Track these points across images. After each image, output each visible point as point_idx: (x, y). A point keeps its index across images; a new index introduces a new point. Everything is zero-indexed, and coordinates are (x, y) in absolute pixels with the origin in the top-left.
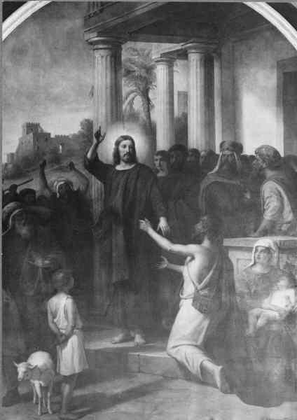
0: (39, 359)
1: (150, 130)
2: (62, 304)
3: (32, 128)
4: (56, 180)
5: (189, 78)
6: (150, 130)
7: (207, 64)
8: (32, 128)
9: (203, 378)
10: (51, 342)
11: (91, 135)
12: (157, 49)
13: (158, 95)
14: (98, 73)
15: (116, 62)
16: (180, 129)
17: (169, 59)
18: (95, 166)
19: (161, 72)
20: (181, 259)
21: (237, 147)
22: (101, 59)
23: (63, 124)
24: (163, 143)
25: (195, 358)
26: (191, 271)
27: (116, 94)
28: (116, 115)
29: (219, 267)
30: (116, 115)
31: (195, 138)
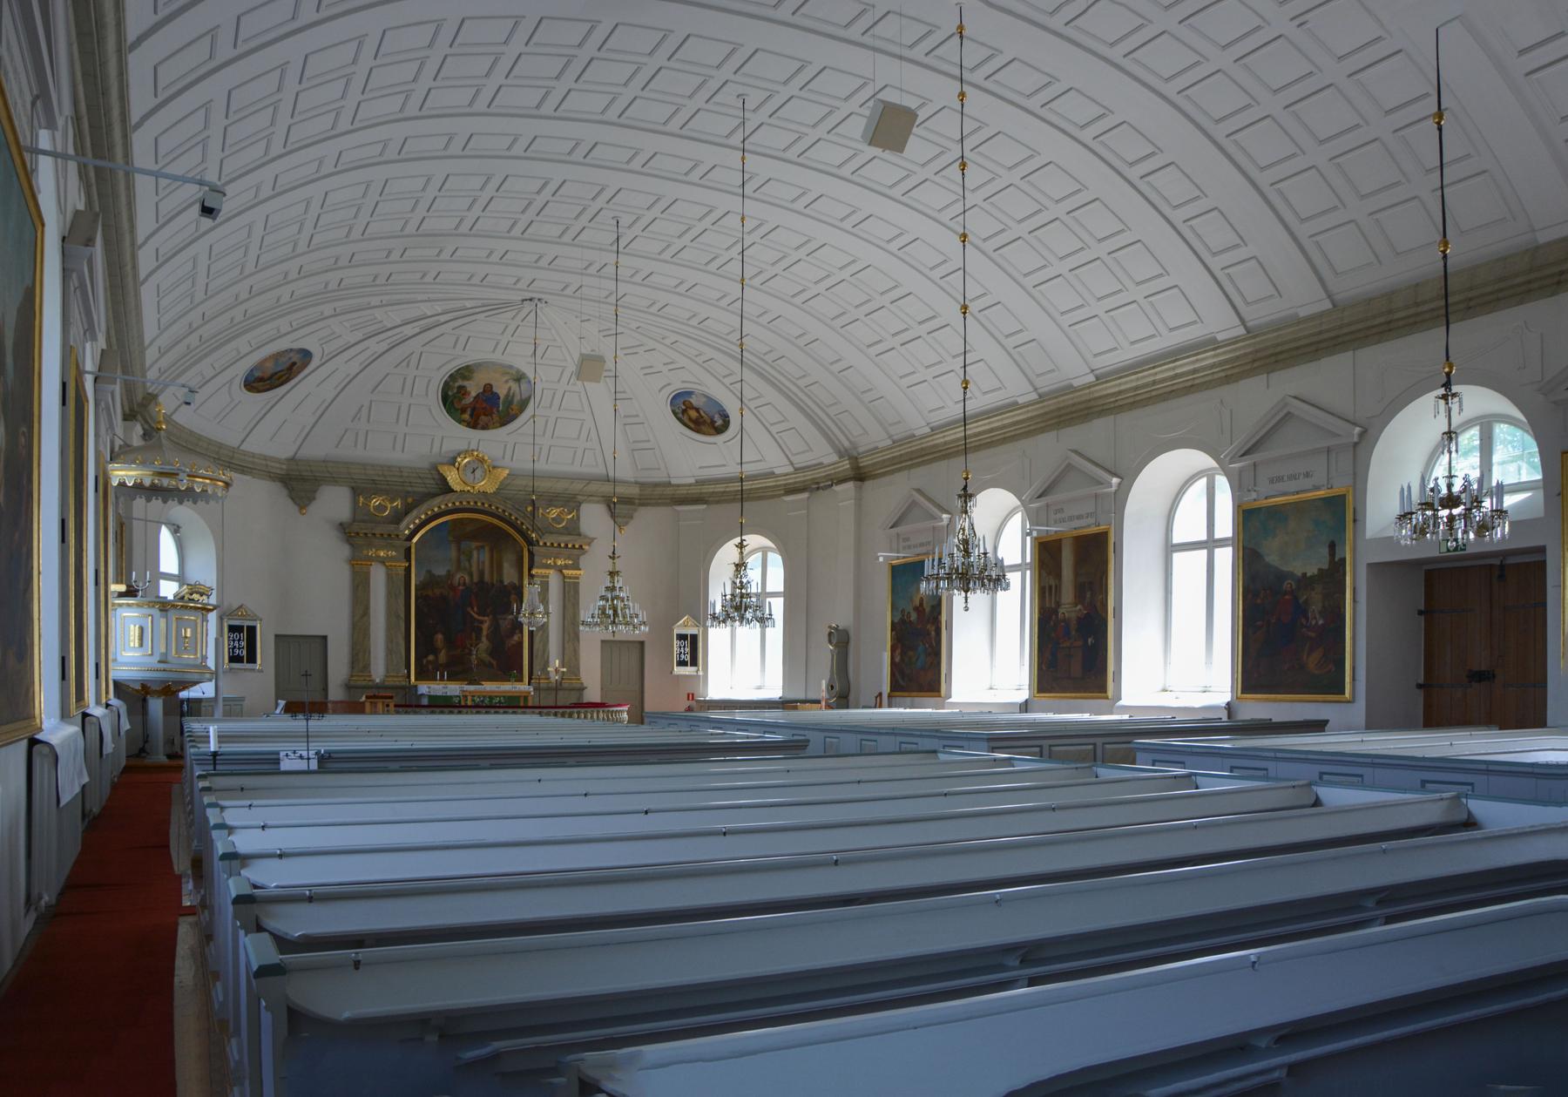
0: (431, 658)
1: (471, 575)
2: (440, 637)
3: (429, 572)
4: (437, 591)
5: (485, 556)
6: (471, 575)
7: (491, 551)
8: (429, 572)
10: (436, 652)
11: (450, 575)
12: (474, 545)
15: (459, 549)
16: (482, 573)
17: (478, 548)
18: (453, 588)
22: (453, 546)
23: (440, 571)
24: (476, 579)
25: (485, 657)
26: (485, 626)
27: (459, 561)
28: (459, 568)
29: (495, 628)
30: (459, 568)
31: (487, 578)
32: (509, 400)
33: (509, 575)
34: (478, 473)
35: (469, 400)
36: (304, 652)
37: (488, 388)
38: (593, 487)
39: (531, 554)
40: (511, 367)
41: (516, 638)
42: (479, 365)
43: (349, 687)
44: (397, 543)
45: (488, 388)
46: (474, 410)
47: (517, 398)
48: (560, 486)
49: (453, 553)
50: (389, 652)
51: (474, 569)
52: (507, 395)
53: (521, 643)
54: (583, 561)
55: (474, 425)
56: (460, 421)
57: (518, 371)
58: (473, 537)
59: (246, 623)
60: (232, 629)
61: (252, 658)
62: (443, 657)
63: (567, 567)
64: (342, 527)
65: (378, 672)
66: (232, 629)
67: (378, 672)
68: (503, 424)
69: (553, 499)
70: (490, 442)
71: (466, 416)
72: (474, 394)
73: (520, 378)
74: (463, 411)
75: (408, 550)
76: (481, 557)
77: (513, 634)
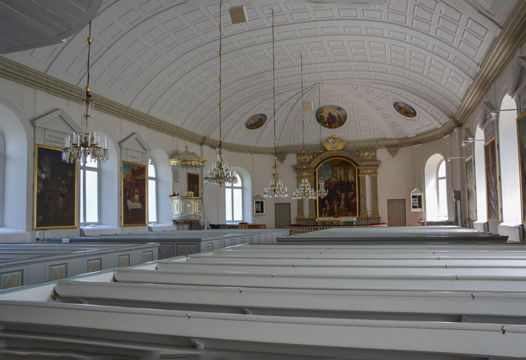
0: (324, 209)
1: (337, 179)
5: (342, 172)
6: (337, 179)
7: (344, 170)
9: (345, 211)
10: (325, 206)
11: (330, 180)
12: (338, 168)
13: (338, 174)
14: (331, 172)
16: (341, 178)
17: (339, 169)
18: (331, 184)
19: (338, 171)
20: (341, 195)
21: (348, 180)
22: (331, 170)
24: (339, 180)
26: (343, 197)
27: (333, 175)
28: (333, 177)
30: (333, 177)
31: (343, 180)
32: (340, 118)
33: (351, 178)
35: (326, 119)
36: (282, 208)
37: (330, 114)
39: (358, 170)
40: (334, 106)
41: (354, 200)
42: (323, 107)
43: (297, 220)
44: (310, 170)
45: (330, 114)
46: (329, 122)
47: (342, 116)
48: (367, 144)
49: (331, 172)
50: (310, 207)
51: (338, 177)
52: (338, 115)
53: (356, 202)
54: (378, 171)
55: (331, 127)
56: (326, 127)
57: (338, 107)
58: (338, 165)
59: (260, 200)
60: (257, 202)
61: (262, 212)
62: (328, 208)
63: (372, 173)
64: (294, 167)
65: (306, 214)
66: (257, 202)
67: (306, 214)
68: (341, 125)
69: (365, 149)
70: (338, 132)
71: (327, 125)
72: (326, 117)
73: (339, 109)
74: (326, 123)
75: (315, 172)
76: (340, 172)
77: (353, 199)
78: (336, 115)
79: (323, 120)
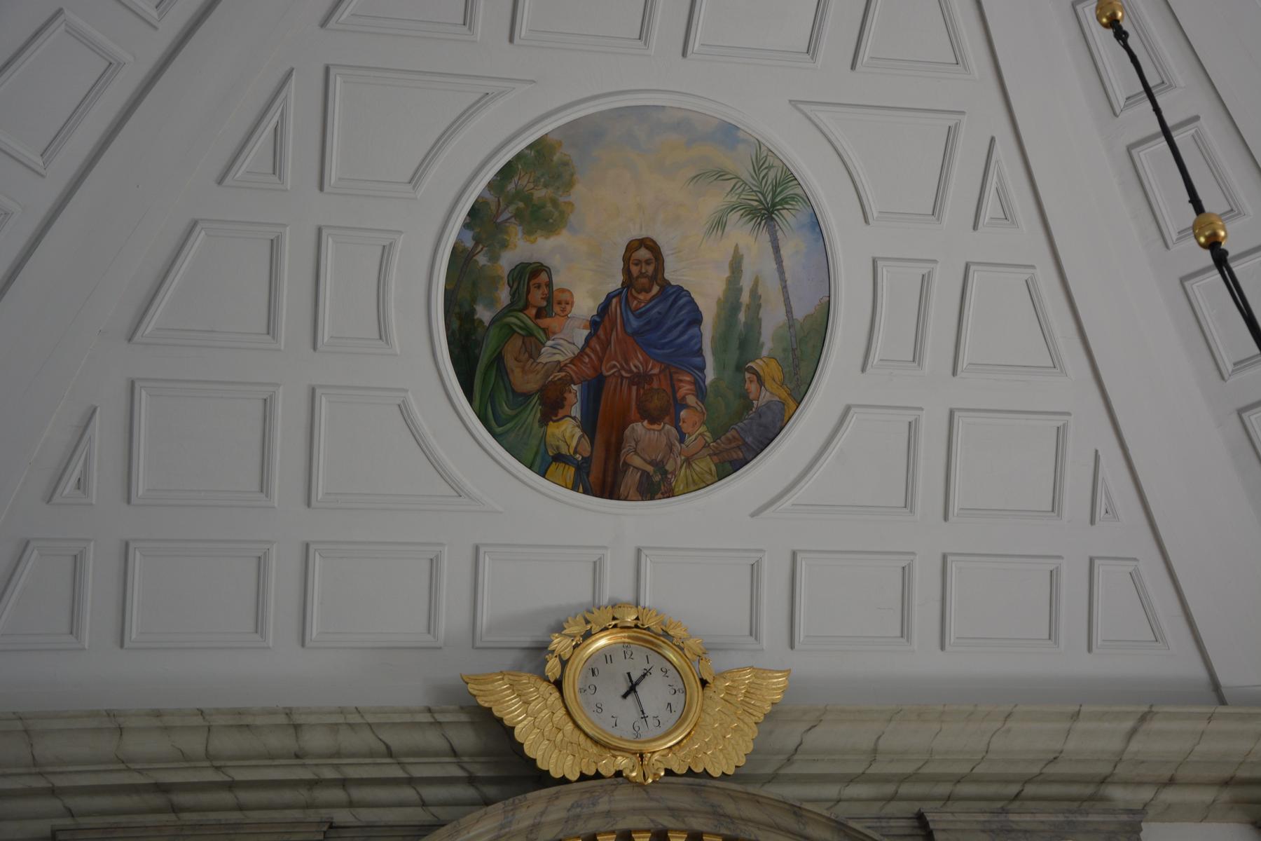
32: (741, 342)
34: (654, 694)
35: (568, 339)
37: (643, 259)
38: (1164, 742)
40: (728, 133)
42: (589, 132)
45: (643, 259)
46: (595, 388)
47: (772, 320)
52: (730, 305)
55: (604, 477)
56: (543, 461)
57: (762, 160)
68: (730, 465)
70: (680, 551)
71: (567, 432)
72: (585, 305)
73: (772, 200)
74: (552, 407)
78: (707, 290)
79: (532, 343)
